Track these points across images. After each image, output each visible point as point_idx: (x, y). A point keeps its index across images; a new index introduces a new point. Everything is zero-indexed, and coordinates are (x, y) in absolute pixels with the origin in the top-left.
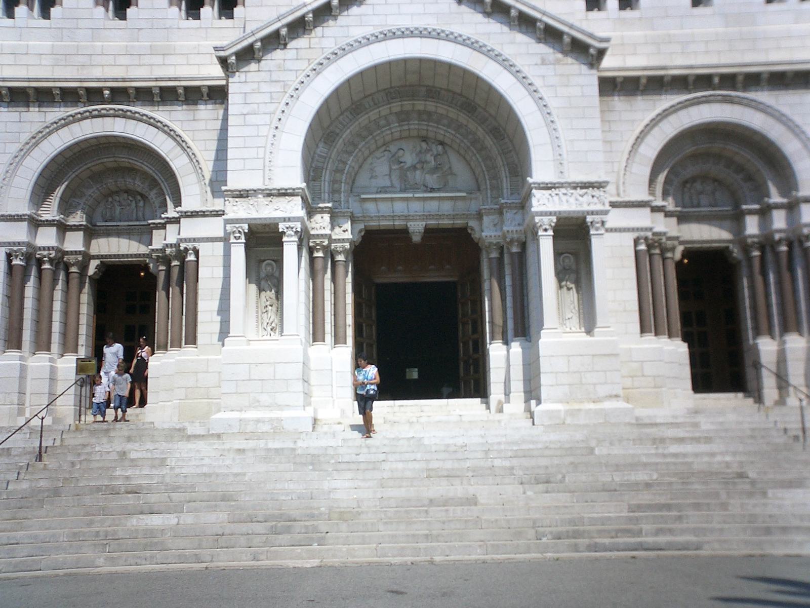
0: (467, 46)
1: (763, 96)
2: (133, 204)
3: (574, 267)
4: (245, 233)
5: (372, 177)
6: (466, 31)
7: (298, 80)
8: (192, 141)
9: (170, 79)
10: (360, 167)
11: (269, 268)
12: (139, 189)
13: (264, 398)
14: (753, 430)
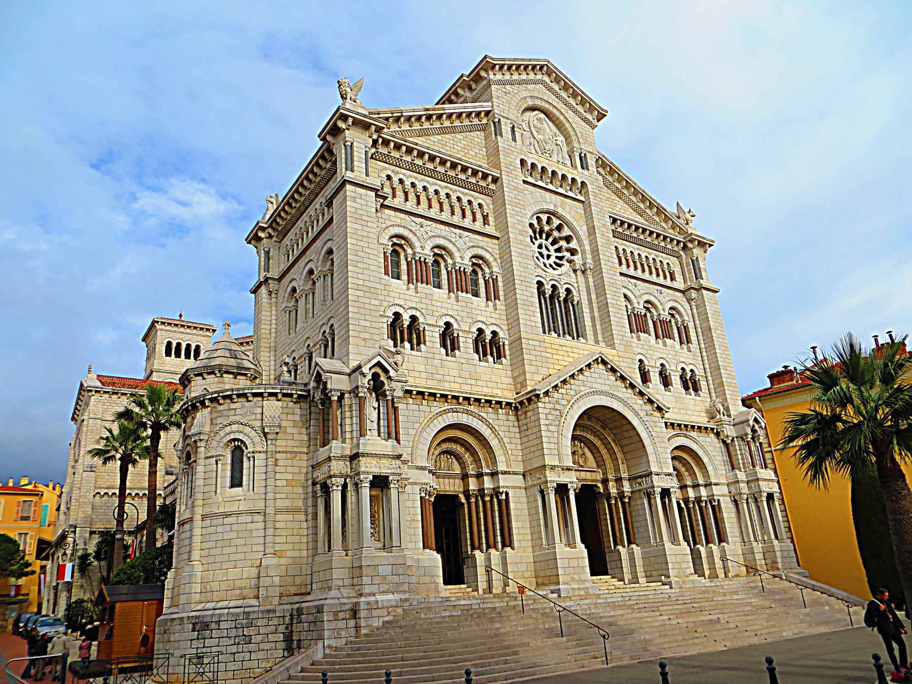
1: (693, 434)
9: (490, 396)
13: (576, 577)
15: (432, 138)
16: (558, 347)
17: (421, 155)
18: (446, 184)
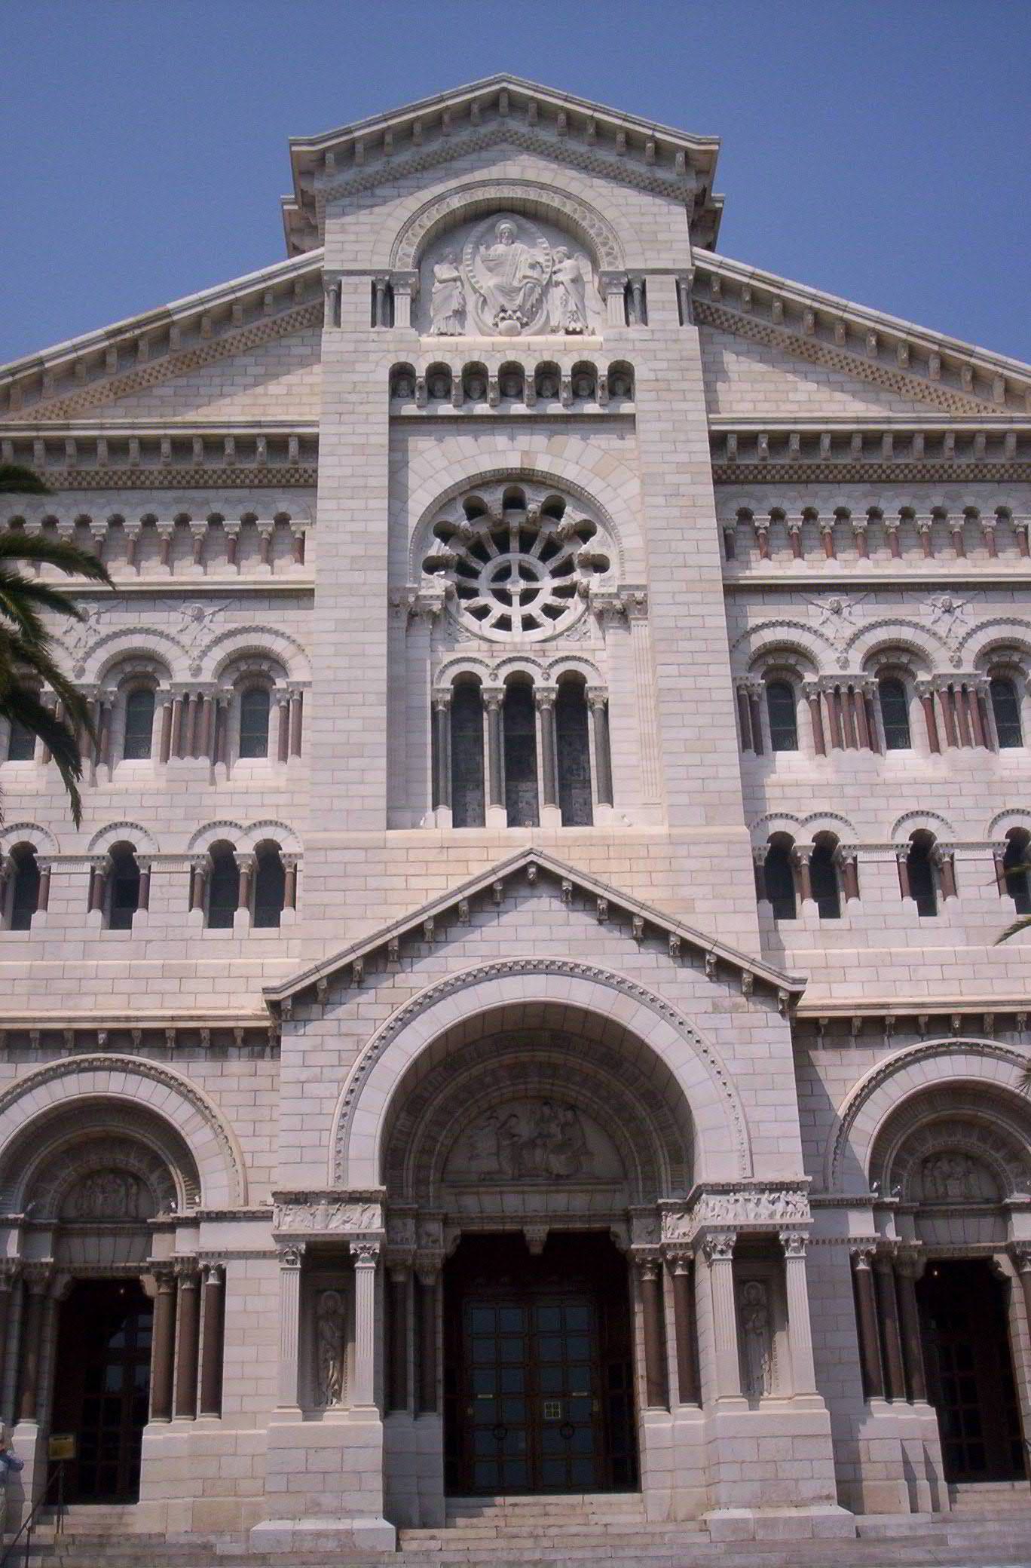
0: (611, 986)
2: (123, 1190)
3: (764, 1300)
4: (301, 1255)
5: (471, 1158)
6: (608, 966)
7: (376, 1035)
8: (220, 1106)
9: (192, 1018)
10: (455, 1142)
11: (331, 1303)
12: (134, 1170)
13: (328, 1501)
14: (1018, 1547)
15: (157, 391)
16: (431, 855)
17: (86, 447)
18: (179, 493)
